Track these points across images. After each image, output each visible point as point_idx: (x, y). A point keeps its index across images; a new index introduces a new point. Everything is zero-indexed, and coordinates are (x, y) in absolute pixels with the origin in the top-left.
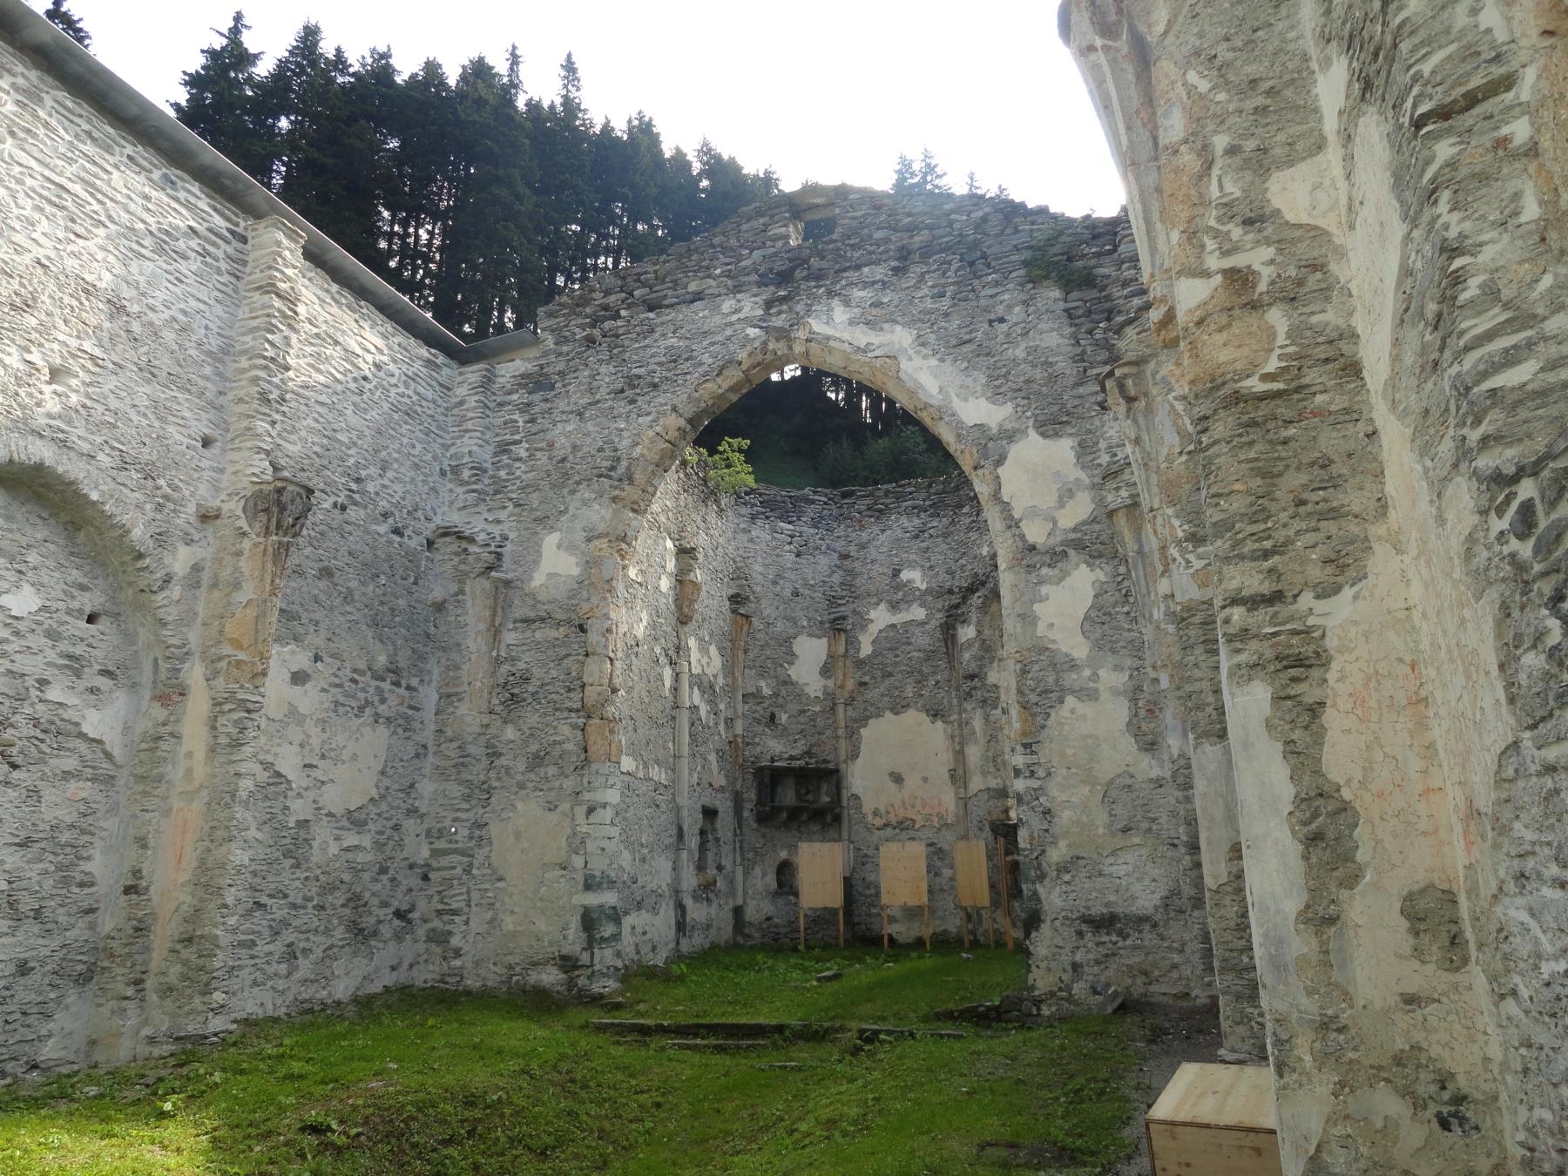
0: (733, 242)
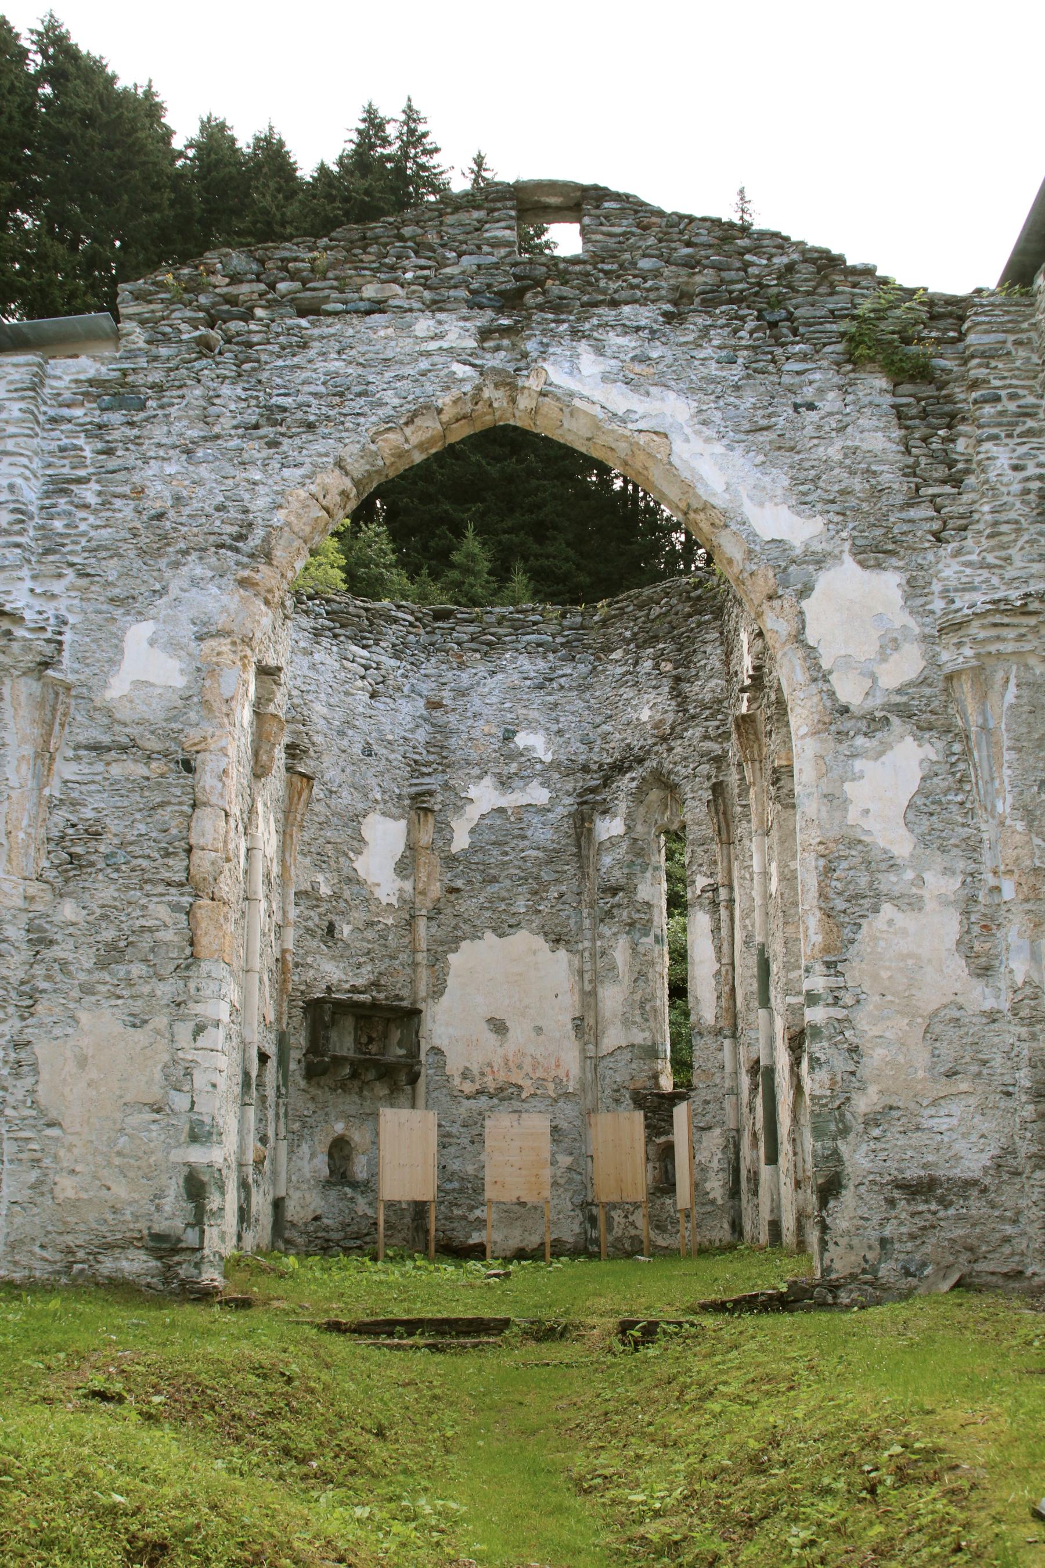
0: (432, 238)
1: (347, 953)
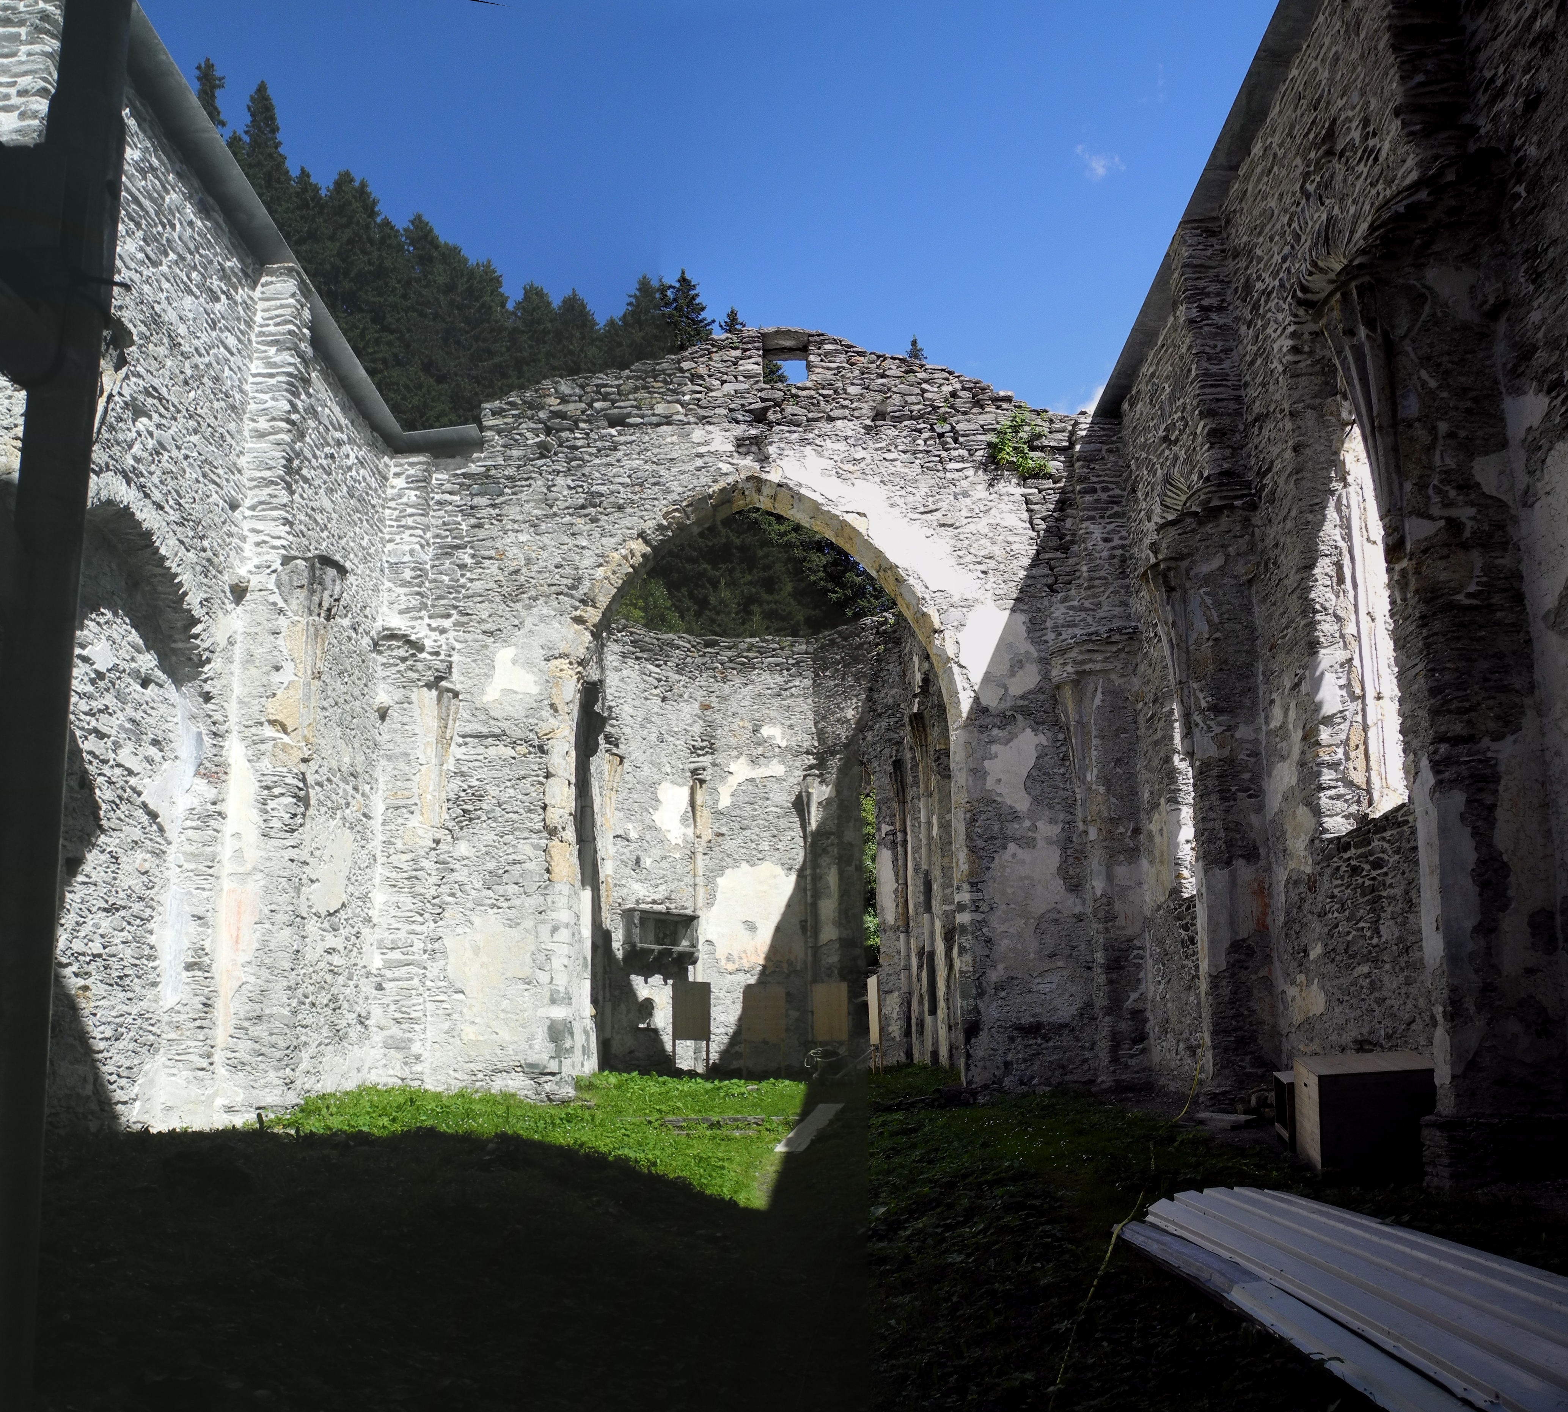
0: (702, 370)
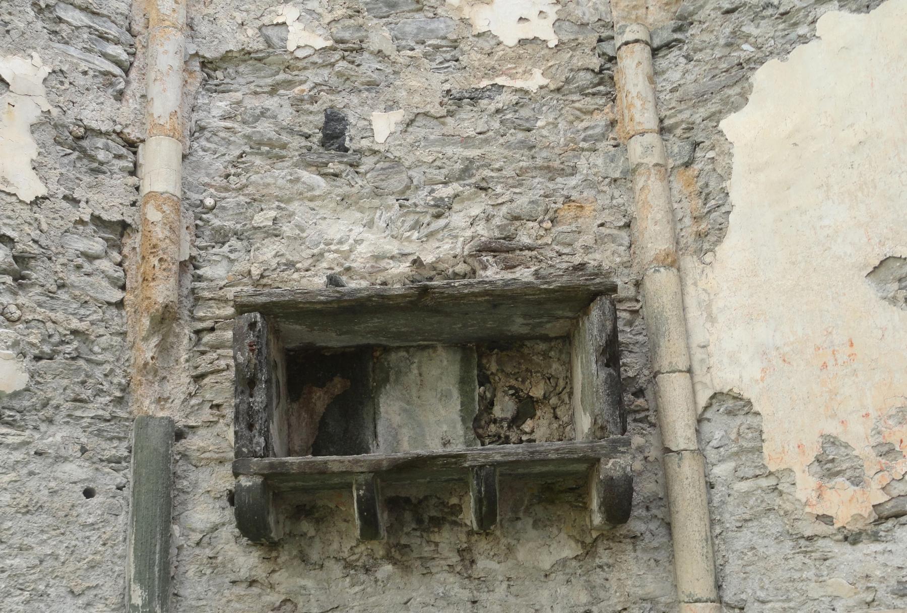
1: (396, 182)
